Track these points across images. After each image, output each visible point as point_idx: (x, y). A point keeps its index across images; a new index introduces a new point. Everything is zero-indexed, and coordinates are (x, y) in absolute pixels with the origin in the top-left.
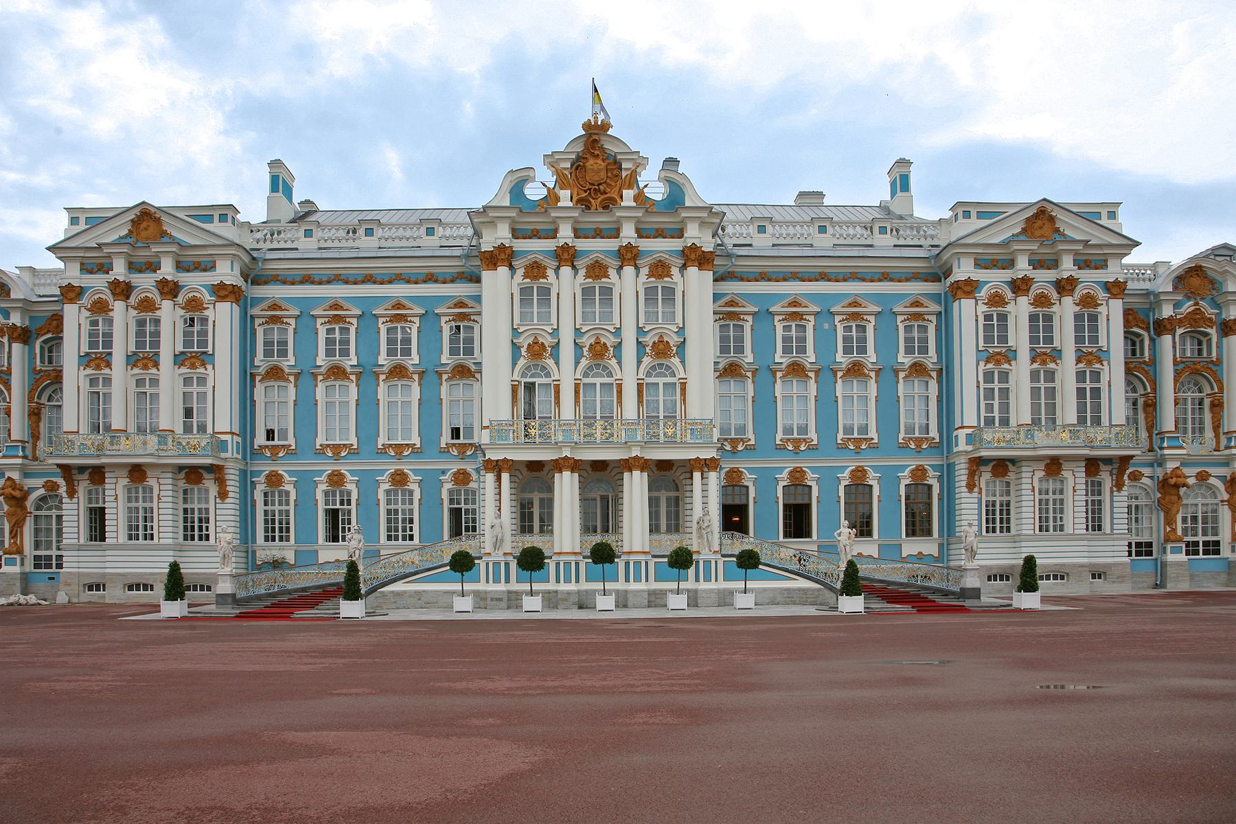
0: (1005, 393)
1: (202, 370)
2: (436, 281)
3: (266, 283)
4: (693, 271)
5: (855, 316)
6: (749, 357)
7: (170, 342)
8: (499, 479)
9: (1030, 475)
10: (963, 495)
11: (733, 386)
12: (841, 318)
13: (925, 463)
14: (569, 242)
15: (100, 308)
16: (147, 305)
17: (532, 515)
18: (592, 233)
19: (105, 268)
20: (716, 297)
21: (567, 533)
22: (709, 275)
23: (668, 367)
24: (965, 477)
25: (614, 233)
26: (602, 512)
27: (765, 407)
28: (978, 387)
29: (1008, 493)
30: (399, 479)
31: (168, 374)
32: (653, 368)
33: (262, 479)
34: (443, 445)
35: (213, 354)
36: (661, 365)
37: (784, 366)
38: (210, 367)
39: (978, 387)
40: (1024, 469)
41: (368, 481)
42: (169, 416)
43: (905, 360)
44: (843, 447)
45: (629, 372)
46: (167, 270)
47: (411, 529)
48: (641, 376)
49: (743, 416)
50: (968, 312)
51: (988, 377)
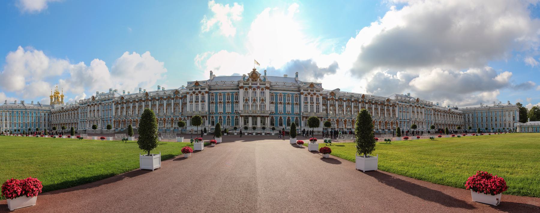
7: (200, 100)
11: (271, 105)
15: (191, 95)
16: (197, 94)
17: (246, 122)
19: (192, 90)
21: (250, 125)
26: (255, 123)
27: (276, 108)
30: (229, 117)
31: (200, 103)
41: (224, 117)
42: (200, 109)
45: (258, 103)
49: (273, 109)
50: (303, 97)
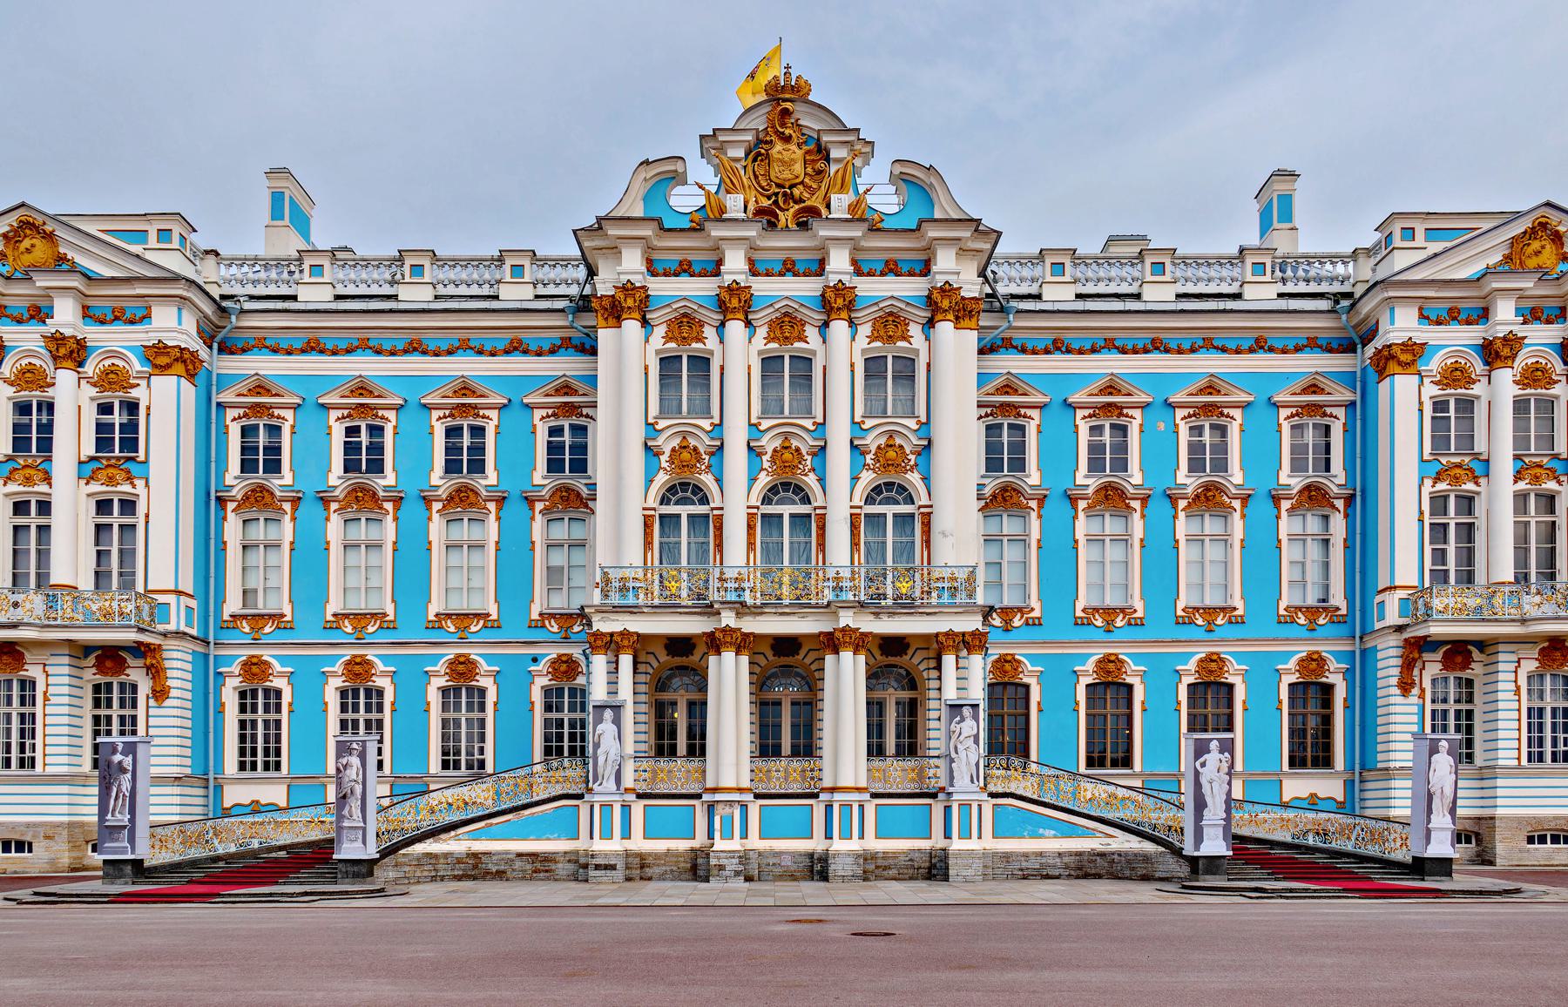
0: (1468, 531)
1: (126, 488)
2: (526, 352)
3: (244, 351)
4: (945, 328)
5: (1209, 409)
6: (1033, 477)
7: (73, 437)
8: (614, 669)
9: (1512, 667)
10: (1392, 700)
12: (1185, 412)
13: (1324, 649)
14: (742, 280)
18: (778, 268)
20: (982, 378)
22: (971, 338)
23: (902, 489)
24: (1396, 671)
25: (814, 267)
28: (1421, 521)
29: (1470, 700)
32: (877, 490)
33: (236, 668)
34: (535, 616)
35: (146, 462)
36: (889, 485)
37: (1090, 491)
38: (140, 483)
39: (1421, 521)
40: (1501, 657)
43: (1292, 481)
44: (1186, 620)
46: (66, 316)
47: (482, 751)
48: (856, 502)
51: (1439, 503)
